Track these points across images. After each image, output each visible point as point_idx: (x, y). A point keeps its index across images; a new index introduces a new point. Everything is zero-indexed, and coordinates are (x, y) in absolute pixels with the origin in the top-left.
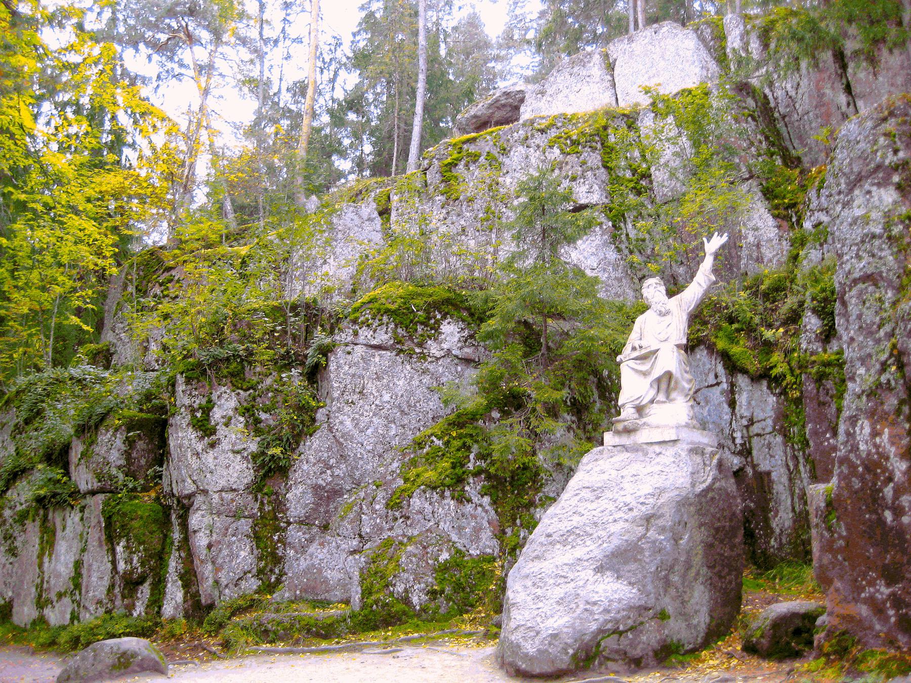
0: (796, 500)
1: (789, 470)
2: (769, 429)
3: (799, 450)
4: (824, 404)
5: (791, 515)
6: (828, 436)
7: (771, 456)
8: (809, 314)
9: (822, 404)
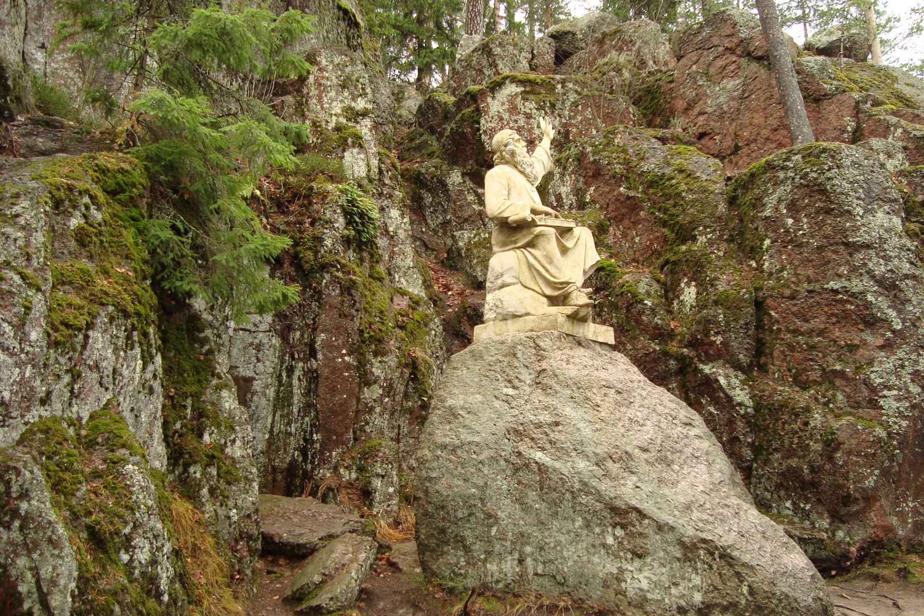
0: (277, 417)
1: (280, 381)
2: (264, 327)
3: (300, 359)
4: (345, 316)
5: (267, 436)
6: (344, 351)
7: (258, 360)
8: (339, 211)
9: (343, 315)
